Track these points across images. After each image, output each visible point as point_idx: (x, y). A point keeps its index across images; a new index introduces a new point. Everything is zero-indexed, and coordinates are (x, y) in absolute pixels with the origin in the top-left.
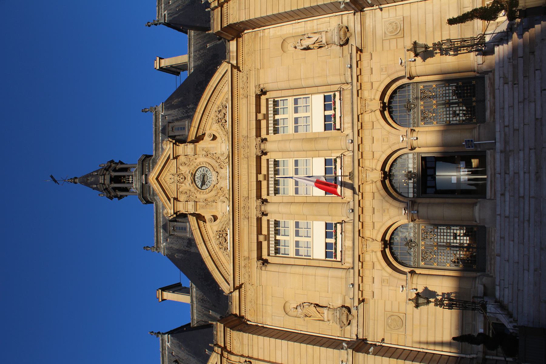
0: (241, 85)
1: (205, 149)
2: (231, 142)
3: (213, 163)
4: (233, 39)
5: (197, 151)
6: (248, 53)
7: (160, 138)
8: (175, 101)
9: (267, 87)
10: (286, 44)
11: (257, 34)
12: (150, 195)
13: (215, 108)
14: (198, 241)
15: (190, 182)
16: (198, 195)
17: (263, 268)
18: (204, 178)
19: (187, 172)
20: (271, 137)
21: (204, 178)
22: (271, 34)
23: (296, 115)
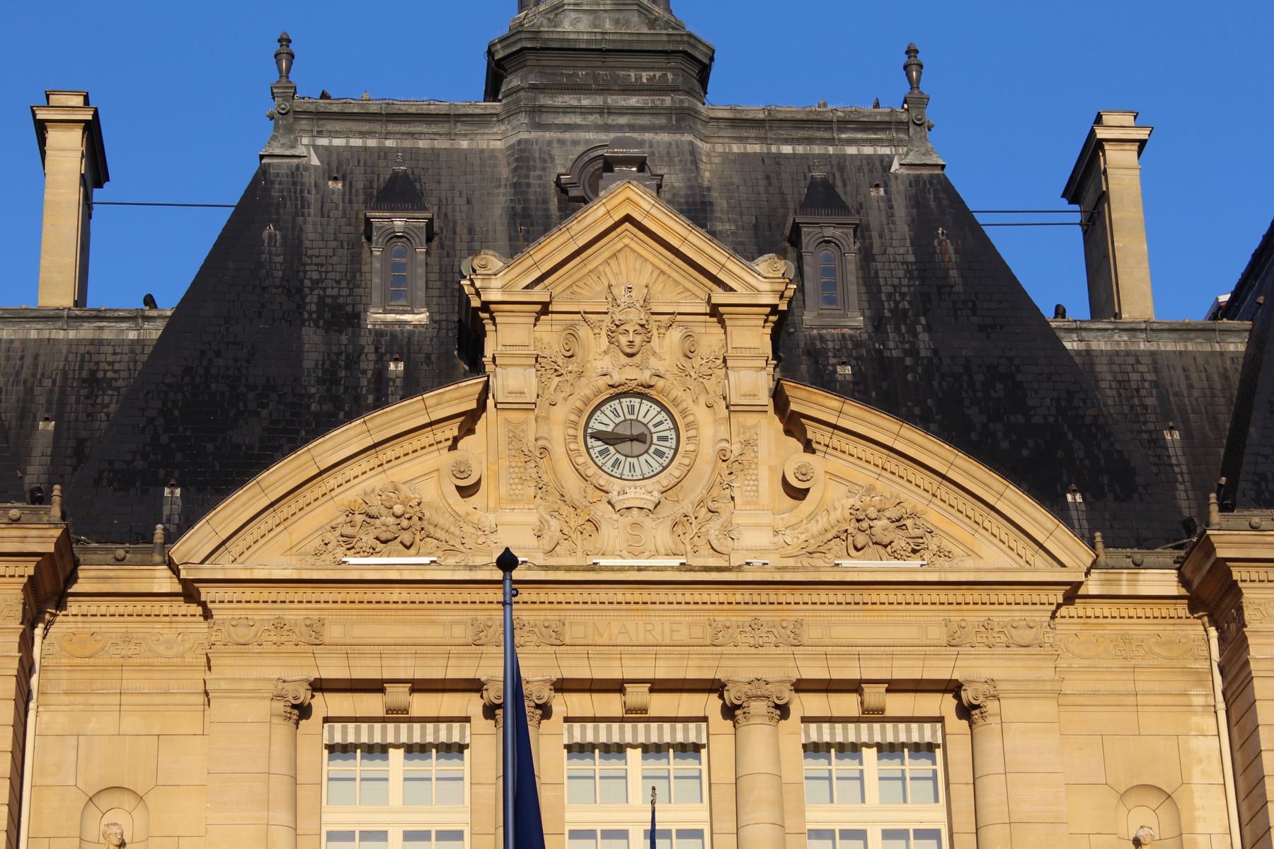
0: (999, 616)
1: (749, 455)
2: (777, 577)
3: (695, 489)
4: (1183, 581)
5: (741, 417)
6: (1126, 639)
7: (787, 149)
8: (947, 247)
9: (989, 730)
10: (1154, 800)
11: (1200, 682)
12: (534, 88)
13: (914, 500)
14: (377, 422)
15: (617, 378)
16: (561, 413)
17: (280, 706)
18: (632, 439)
19: (655, 363)
20: (794, 734)
21: (632, 439)
22: (1197, 744)
23: (874, 836)
